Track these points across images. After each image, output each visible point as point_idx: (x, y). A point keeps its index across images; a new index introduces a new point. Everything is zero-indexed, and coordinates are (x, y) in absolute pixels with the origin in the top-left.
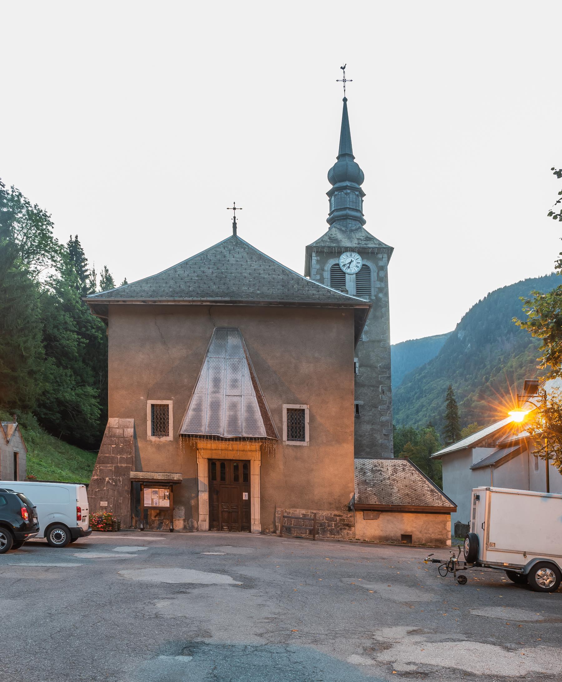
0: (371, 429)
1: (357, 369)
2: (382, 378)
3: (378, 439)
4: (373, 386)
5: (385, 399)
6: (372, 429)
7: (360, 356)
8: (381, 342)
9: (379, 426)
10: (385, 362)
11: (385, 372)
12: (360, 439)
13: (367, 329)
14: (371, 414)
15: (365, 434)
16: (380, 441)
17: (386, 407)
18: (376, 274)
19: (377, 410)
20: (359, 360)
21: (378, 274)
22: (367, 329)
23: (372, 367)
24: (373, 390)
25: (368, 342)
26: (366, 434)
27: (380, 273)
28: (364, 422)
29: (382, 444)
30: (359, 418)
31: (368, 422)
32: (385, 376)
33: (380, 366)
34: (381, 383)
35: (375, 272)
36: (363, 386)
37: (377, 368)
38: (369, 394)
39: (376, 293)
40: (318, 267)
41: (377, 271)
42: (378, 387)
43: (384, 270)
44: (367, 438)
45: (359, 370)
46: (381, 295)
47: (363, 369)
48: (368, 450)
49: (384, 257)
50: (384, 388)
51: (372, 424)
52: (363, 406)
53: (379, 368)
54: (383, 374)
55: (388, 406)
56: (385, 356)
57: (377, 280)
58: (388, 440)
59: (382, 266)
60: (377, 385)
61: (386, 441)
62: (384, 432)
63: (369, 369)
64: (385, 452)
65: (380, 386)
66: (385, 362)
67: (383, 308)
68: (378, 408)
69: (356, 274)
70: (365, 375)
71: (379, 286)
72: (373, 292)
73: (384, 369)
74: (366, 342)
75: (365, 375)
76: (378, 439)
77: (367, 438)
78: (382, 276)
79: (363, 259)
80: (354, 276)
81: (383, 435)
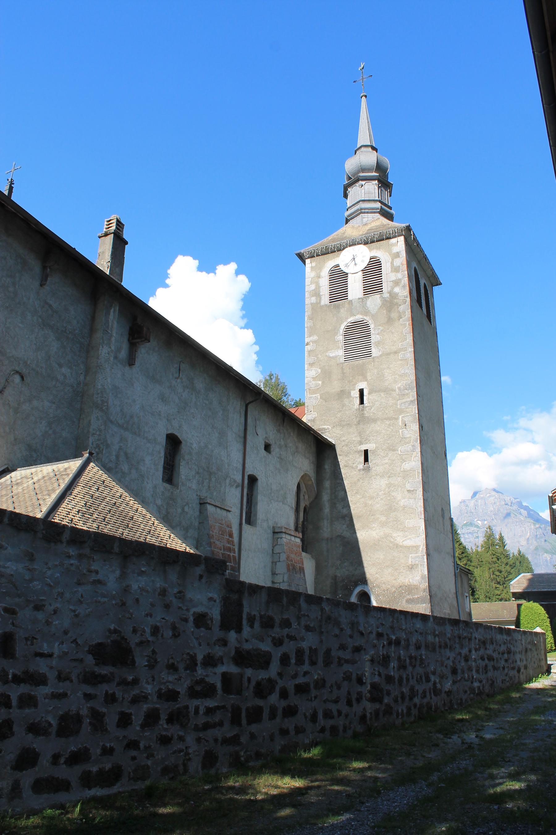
0: (387, 484)
1: (365, 398)
2: (403, 405)
3: (399, 498)
4: (389, 419)
5: (408, 436)
6: (389, 485)
7: (369, 378)
8: (399, 353)
9: (399, 479)
10: (406, 380)
11: (407, 394)
12: (370, 503)
13: (379, 339)
14: (386, 461)
15: (378, 494)
16: (402, 503)
17: (410, 446)
18: (389, 264)
19: (396, 453)
20: (368, 384)
21: (392, 263)
22: (379, 339)
23: (387, 391)
24: (389, 425)
25: (381, 356)
26: (380, 493)
27: (395, 261)
28: (377, 475)
29: (404, 507)
30: (369, 470)
31: (382, 476)
32: (408, 400)
33: (399, 388)
34: (401, 411)
35: (389, 262)
36: (375, 421)
37: (395, 391)
38: (383, 431)
39: (389, 289)
40: (313, 274)
41: (390, 260)
42: (397, 419)
43: (401, 256)
44: (382, 499)
45: (368, 399)
46: (397, 290)
47: (374, 396)
48: (383, 519)
49: (398, 241)
50: (406, 419)
51: (389, 477)
52: (374, 452)
53: (397, 390)
54: (403, 399)
55: (413, 446)
56: (407, 371)
57: (392, 271)
58: (415, 499)
59: (398, 253)
60: (396, 417)
61: (412, 501)
62: (408, 486)
63: (382, 394)
64: (410, 519)
65: (400, 417)
66: (406, 380)
67: (400, 305)
68: (398, 450)
69: (362, 270)
70: (377, 404)
71: (394, 278)
72: (386, 287)
73: (406, 391)
74: (377, 357)
75: (377, 404)
76: (399, 498)
77: (382, 499)
78: (398, 265)
79: (370, 250)
80: (361, 274)
81: (406, 493)
